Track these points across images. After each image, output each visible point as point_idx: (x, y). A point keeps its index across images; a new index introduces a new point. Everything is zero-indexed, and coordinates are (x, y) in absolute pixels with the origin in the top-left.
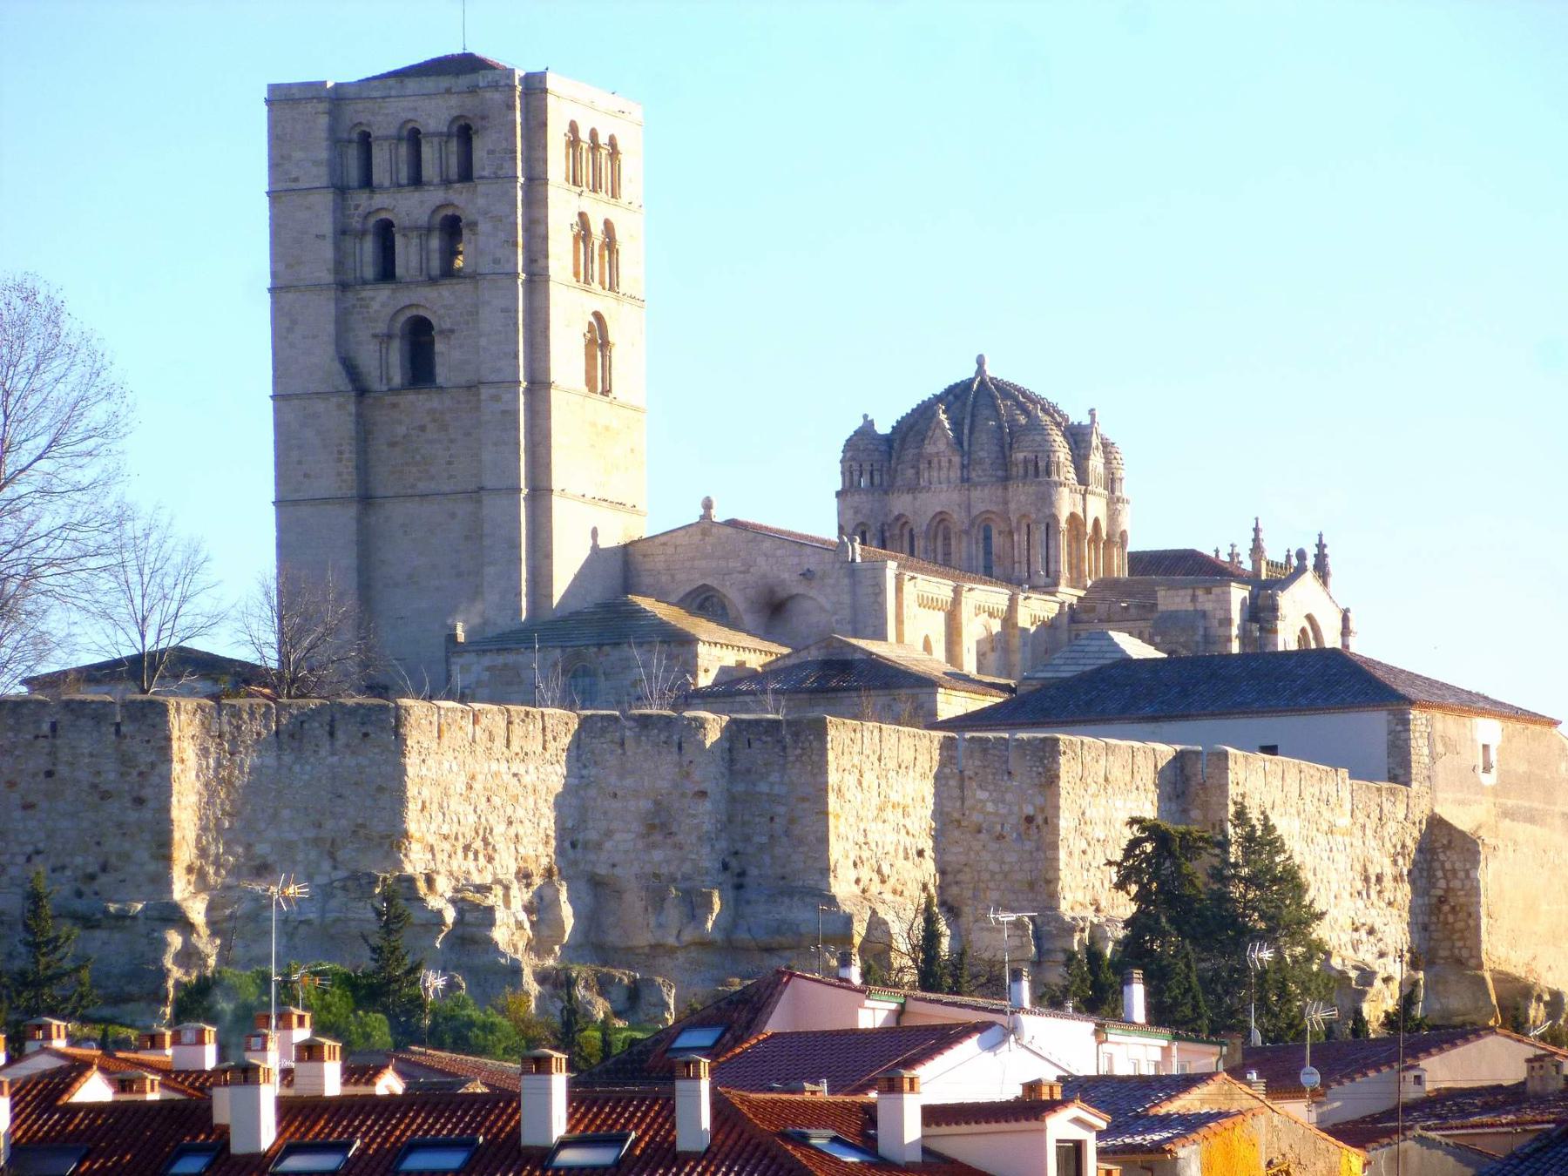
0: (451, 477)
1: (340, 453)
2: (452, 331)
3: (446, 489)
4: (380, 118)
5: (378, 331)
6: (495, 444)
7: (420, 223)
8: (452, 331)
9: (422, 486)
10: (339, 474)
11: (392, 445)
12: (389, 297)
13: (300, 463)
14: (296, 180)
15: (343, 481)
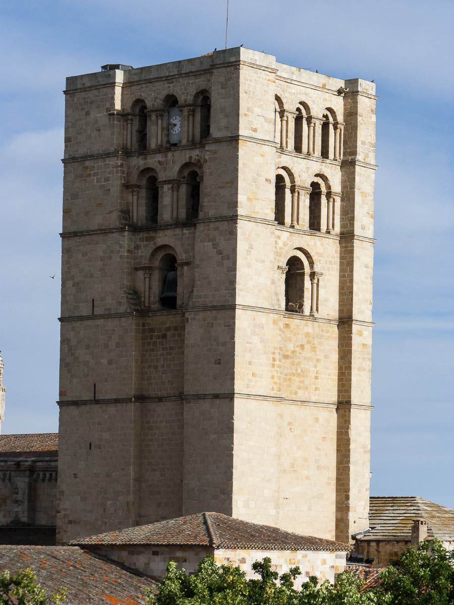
0: (316, 389)
1: (274, 360)
2: (322, 274)
3: (314, 399)
4: (287, 95)
5: (280, 264)
6: (359, 369)
7: (306, 186)
8: (322, 274)
9: (302, 395)
10: (273, 378)
11: (286, 357)
12: (288, 238)
13: (250, 363)
14: (255, 130)
15: (275, 383)
